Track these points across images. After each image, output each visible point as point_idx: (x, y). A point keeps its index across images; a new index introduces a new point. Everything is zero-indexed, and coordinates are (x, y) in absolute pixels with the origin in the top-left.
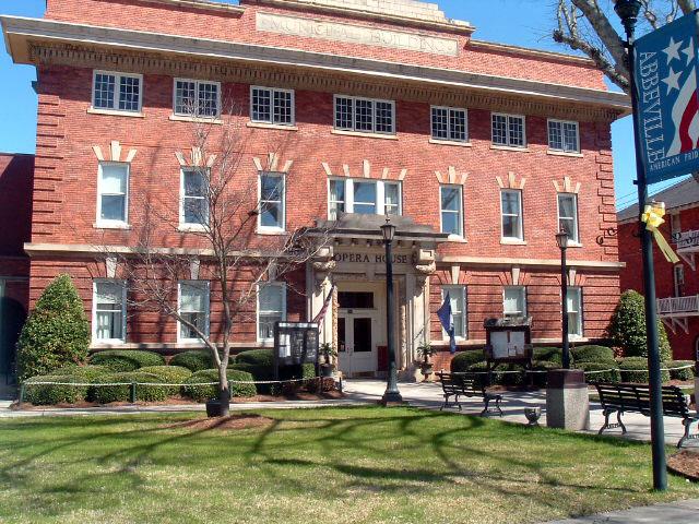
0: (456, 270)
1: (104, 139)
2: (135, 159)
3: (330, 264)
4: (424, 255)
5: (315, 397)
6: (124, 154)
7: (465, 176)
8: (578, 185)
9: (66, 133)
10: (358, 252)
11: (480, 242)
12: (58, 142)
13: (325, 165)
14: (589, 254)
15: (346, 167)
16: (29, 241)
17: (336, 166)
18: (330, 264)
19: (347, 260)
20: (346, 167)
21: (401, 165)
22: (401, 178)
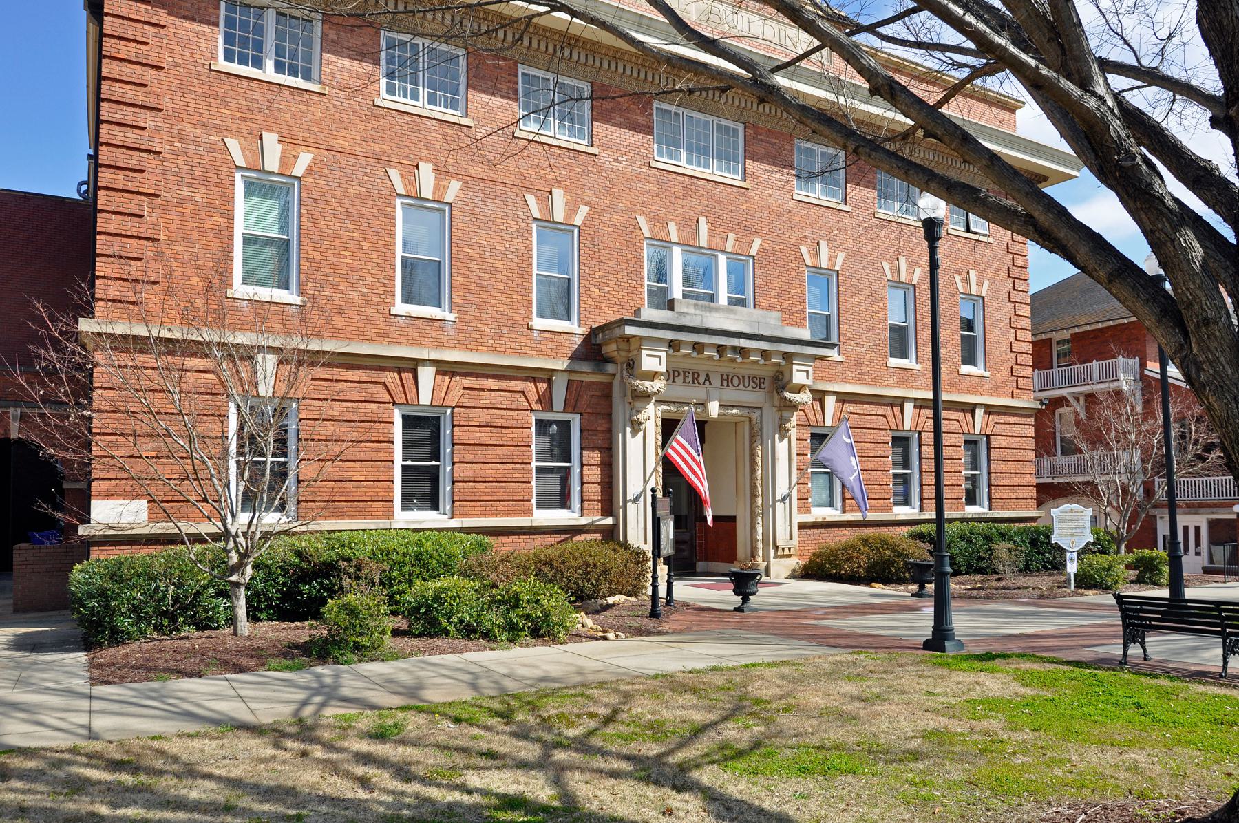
0: (426, 375)
1: (246, 126)
2: (309, 172)
3: (657, 385)
4: (798, 378)
5: (1064, 499)
6: (287, 161)
7: (841, 257)
8: (986, 284)
9: (166, 103)
10: (695, 367)
11: (859, 362)
12: (149, 119)
13: (642, 220)
14: (997, 389)
15: (672, 227)
16: (89, 313)
17: (655, 220)
18: (657, 385)
19: (679, 380)
20: (672, 227)
21: (752, 232)
22: (753, 252)
